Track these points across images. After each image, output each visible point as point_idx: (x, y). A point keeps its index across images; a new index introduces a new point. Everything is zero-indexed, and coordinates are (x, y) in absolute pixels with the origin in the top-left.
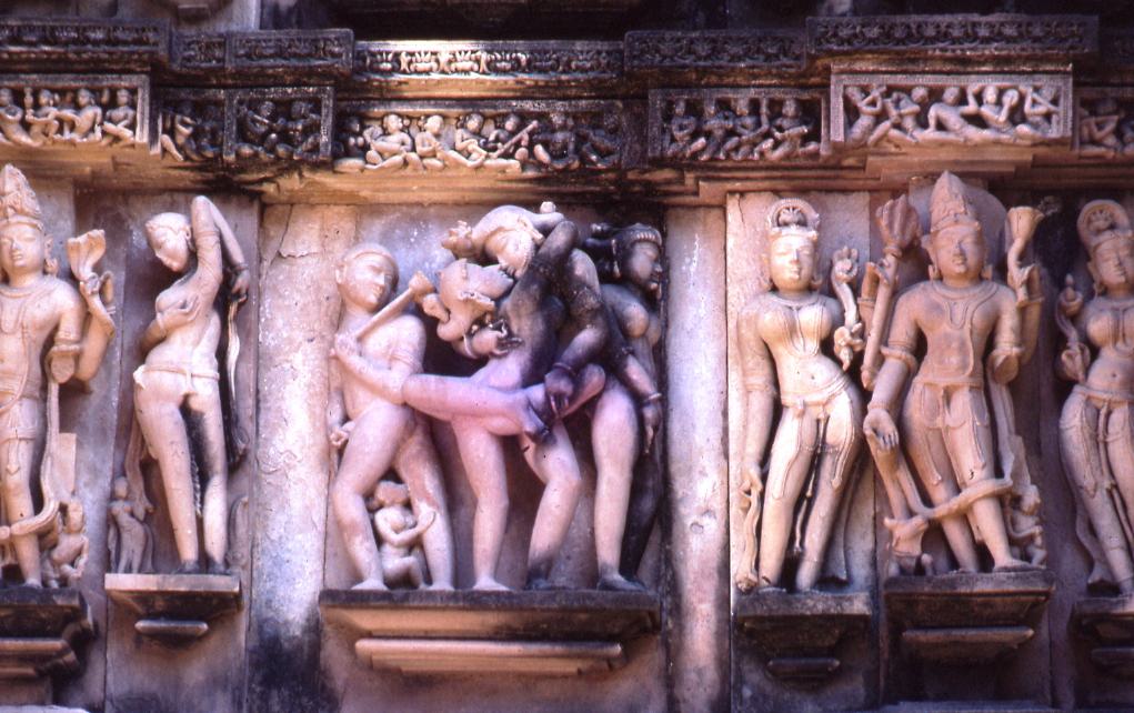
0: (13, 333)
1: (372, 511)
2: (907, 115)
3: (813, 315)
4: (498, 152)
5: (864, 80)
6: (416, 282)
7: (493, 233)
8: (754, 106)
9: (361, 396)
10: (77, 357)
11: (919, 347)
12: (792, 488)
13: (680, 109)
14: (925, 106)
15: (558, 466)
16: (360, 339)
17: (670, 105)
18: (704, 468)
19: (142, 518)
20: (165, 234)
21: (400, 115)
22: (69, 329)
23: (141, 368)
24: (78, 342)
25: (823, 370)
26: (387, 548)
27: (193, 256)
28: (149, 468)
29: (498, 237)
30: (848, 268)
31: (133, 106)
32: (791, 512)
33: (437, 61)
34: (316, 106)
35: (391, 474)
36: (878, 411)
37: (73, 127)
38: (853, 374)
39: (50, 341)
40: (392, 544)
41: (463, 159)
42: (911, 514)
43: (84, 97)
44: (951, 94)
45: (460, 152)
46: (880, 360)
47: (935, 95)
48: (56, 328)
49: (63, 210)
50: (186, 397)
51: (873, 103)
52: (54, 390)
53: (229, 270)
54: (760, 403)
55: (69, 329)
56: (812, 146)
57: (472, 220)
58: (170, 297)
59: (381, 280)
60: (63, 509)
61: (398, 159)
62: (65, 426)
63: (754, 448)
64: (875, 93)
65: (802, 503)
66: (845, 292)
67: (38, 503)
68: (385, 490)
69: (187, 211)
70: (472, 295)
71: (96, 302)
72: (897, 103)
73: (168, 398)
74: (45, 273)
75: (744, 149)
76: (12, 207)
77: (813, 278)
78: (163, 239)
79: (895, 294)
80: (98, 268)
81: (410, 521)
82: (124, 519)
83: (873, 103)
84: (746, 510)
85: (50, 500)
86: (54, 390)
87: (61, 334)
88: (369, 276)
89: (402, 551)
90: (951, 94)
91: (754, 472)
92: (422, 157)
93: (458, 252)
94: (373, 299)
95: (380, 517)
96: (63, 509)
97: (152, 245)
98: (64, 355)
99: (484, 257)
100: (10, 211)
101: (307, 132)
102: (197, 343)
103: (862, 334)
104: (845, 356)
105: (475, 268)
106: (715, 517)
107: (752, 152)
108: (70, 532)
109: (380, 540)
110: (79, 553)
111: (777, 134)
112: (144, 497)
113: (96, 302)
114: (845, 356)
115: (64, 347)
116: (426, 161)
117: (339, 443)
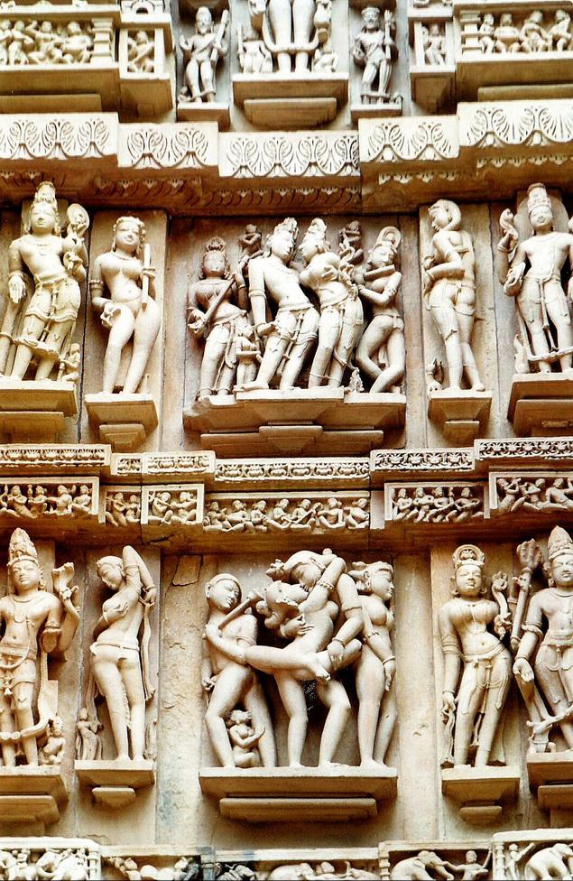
1: (228, 727)
2: (533, 494)
3: (483, 607)
4: (298, 521)
5: (509, 475)
6: (252, 596)
7: (296, 566)
8: (445, 491)
9: (221, 662)
11: (544, 624)
13: (402, 493)
14: (543, 488)
15: (337, 698)
16: (222, 627)
17: (397, 491)
19: (95, 731)
21: (241, 501)
22: (53, 621)
23: (95, 644)
25: (490, 638)
26: (237, 748)
27: (124, 579)
28: (101, 701)
29: (298, 569)
31: (90, 495)
32: (472, 721)
33: (263, 470)
34: (195, 493)
35: (240, 705)
36: (521, 661)
37: (55, 505)
38: (506, 642)
39: (43, 627)
40: (240, 746)
41: (277, 525)
42: (543, 720)
43: (62, 489)
44: (558, 483)
45: (276, 520)
46: (522, 632)
47: (549, 483)
48: (46, 620)
49: (49, 556)
50: (121, 659)
51: (514, 488)
53: (144, 589)
54: (453, 661)
55: (53, 621)
56: (479, 513)
57: (285, 556)
58: (111, 605)
59: (232, 595)
60: (51, 723)
61: (241, 525)
63: (450, 686)
64: (515, 482)
65: (477, 716)
66: (500, 597)
67: (37, 719)
68: (238, 715)
69: (120, 555)
72: (527, 488)
73: (109, 660)
74: (39, 589)
75: (439, 517)
77: (481, 590)
79: (528, 597)
80: (69, 585)
81: (250, 732)
82: (85, 732)
83: (514, 488)
84: (445, 722)
88: (227, 591)
89: (247, 750)
90: (558, 483)
91: (450, 698)
92: (255, 525)
93: (275, 577)
94: (228, 606)
95: (233, 730)
96: (51, 723)
97: (100, 575)
98: (50, 635)
99: (291, 579)
100: (19, 553)
101: (189, 509)
103: (510, 618)
104: (502, 632)
105: (286, 586)
107: (444, 518)
108: (55, 736)
109: (233, 743)
110: (60, 748)
111: (459, 508)
113: (69, 604)
114: (502, 632)
115: (51, 630)
116: (257, 527)
117: (209, 689)
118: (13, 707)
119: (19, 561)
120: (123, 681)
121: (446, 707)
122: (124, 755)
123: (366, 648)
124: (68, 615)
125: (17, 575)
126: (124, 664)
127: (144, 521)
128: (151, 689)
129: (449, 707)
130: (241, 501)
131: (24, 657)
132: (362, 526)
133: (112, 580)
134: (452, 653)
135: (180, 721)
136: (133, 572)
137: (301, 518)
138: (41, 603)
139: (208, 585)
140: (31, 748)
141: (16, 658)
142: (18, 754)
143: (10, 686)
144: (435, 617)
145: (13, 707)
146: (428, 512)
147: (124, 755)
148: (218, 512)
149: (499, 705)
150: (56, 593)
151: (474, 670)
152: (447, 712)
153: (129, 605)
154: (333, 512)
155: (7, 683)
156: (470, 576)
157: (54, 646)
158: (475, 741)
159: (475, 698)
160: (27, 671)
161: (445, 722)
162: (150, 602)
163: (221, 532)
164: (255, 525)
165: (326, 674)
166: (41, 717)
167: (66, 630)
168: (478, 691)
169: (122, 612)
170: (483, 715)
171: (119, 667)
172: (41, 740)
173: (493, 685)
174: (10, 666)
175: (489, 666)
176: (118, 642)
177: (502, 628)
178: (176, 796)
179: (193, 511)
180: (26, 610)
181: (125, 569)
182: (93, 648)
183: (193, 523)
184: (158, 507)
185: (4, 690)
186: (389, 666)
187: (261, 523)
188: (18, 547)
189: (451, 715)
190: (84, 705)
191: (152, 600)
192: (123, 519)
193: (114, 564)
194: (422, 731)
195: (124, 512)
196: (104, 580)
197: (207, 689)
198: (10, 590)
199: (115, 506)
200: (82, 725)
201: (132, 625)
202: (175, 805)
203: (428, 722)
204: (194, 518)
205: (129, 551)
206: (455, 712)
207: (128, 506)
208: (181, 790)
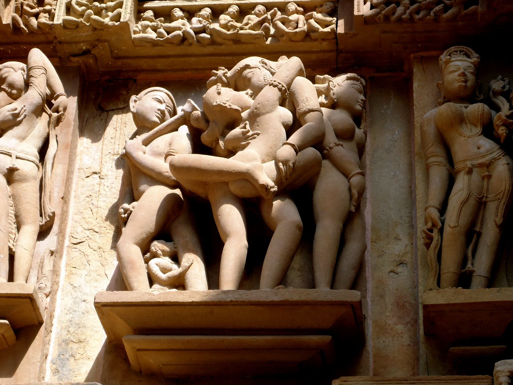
1: (147, 261)
12: (464, 220)
18: (398, 235)
21: (182, 9)
25: (486, 144)
29: (246, 72)
30: (502, 86)
54: (438, 175)
65: (471, 235)
69: (23, 58)
70: (225, 104)
91: (435, 214)
101: (113, 9)
102: (22, 138)
106: (407, 267)
107: (429, 14)
117: (126, 215)
121: (430, 225)
123: (326, 163)
127: (58, 20)
128: (49, 209)
129: (434, 225)
130: (182, 9)
132: (328, 29)
134: (439, 164)
135: (90, 258)
137: (252, 23)
139: (133, 97)
144: (417, 134)
146: (408, 8)
148: (151, 21)
149: (499, 220)
151: (466, 177)
152: (431, 230)
154: (293, 17)
156: (462, 70)
158: (469, 265)
159: (468, 209)
161: (428, 246)
162: (58, 112)
163: (153, 43)
164: (197, 32)
165: (271, 183)
168: (472, 201)
170: (479, 234)
173: (491, 196)
175: (487, 173)
177: (503, 128)
178: (75, 346)
179: (115, 12)
183: (117, 24)
184: (77, 7)
186: (356, 180)
187: (204, 30)
189: (435, 234)
192: (34, 21)
194: (400, 269)
195: (36, 16)
197: (123, 216)
199: (25, 7)
202: (72, 356)
203: (408, 259)
204: (117, 18)
205: (37, 56)
206: (441, 231)
207: (41, 8)
208: (82, 337)
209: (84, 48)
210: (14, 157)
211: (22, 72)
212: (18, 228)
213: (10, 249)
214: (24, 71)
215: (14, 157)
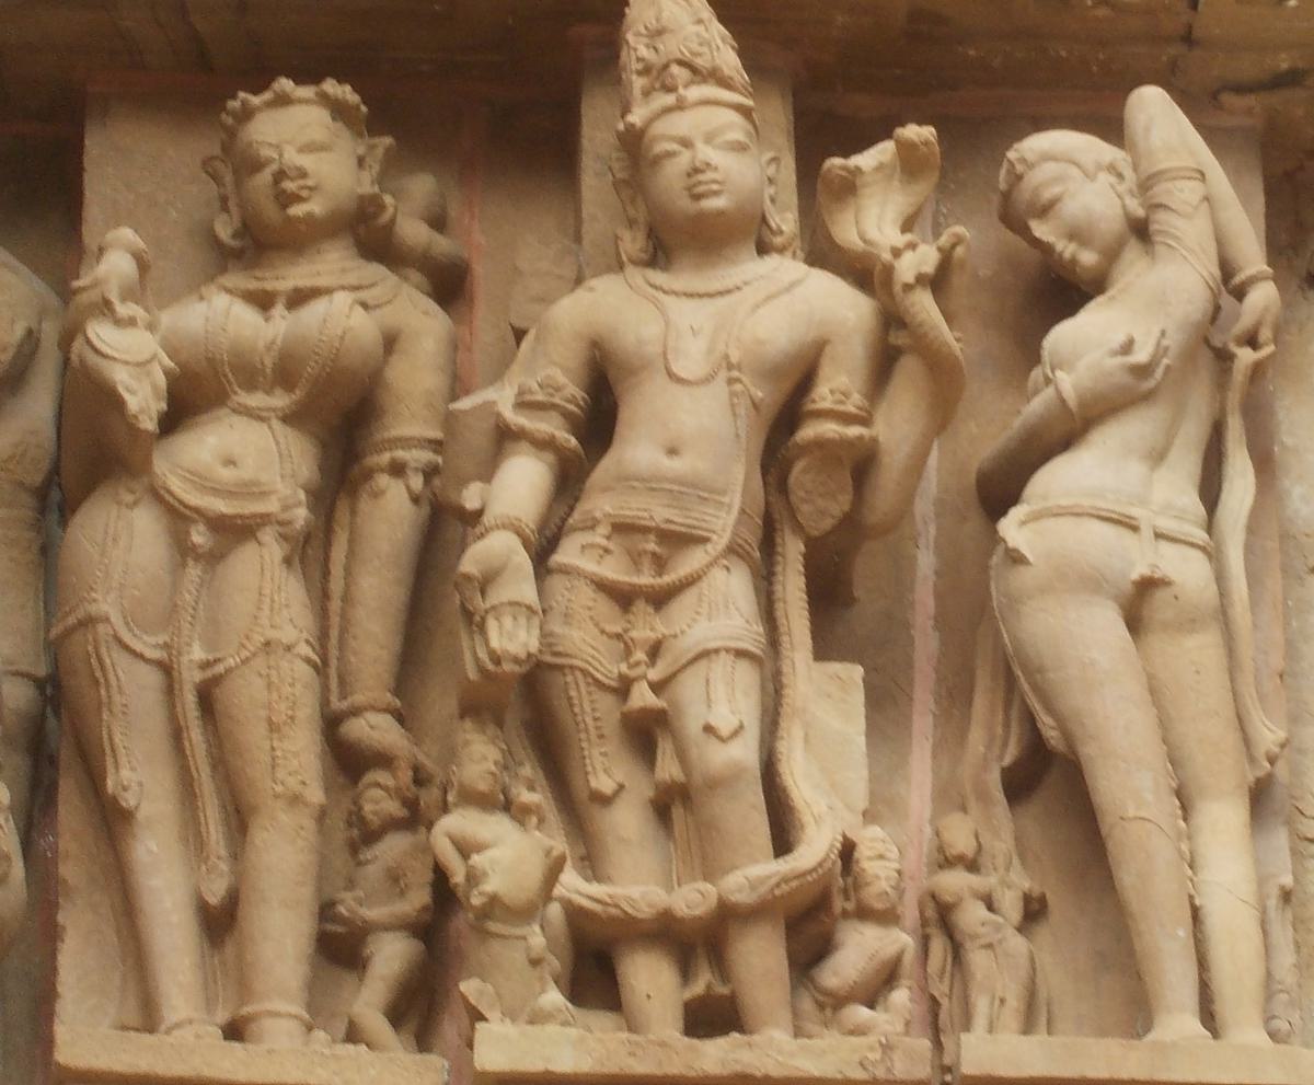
0: (708, 379)
10: (862, 464)
20: (1058, 179)
23: (1016, 513)
24: (865, 421)
27: (1140, 230)
48: (805, 381)
50: (1148, 586)
52: (793, 550)
55: (838, 385)
58: (1085, 344)
60: (848, 851)
62: (824, 649)
67: (783, 832)
71: (924, 306)
73: (1091, 582)
74: (763, 249)
76: (681, 63)
78: (1056, 190)
82: (972, 916)
85: (818, 820)
86: (793, 550)
87: (824, 394)
96: (848, 851)
102: (1157, 456)
108: (864, 914)
112: (1016, 861)
113: (924, 306)
115: (830, 429)
118: (668, 768)
119: (680, 106)
120: (1154, 691)
122: (1179, 1023)
124: (909, 372)
125: (671, 177)
126: (1160, 607)
128: (1268, 734)
131: (720, 542)
133: (1076, 235)
136: (1185, 193)
138: (786, 301)
140: (760, 959)
141: (678, 540)
142: (698, 988)
143: (655, 674)
145: (668, 768)
147: (1179, 1023)
150: (863, 272)
153: (1173, 341)
155: (640, 655)
157: (841, 504)
160: (720, 609)
162: (1252, 341)
166: (806, 817)
167: (896, 426)
169: (1142, 371)
171: (1135, 622)
172: (808, 923)
174: (646, 579)
176: (1107, 506)
180: (715, 335)
181: (1145, 185)
182: (1012, 528)
185: (623, 689)
188: (671, 47)
190: (948, 797)
191: (1265, 334)
193: (1088, 160)
196: (1040, 230)
198: (632, 243)
200: (954, 882)
201: (1178, 441)
209: (1284, 66)
210: (1147, 532)
211: (1113, 179)
212: (1186, 810)
213: (1191, 897)
214: (1120, 176)
215: (1147, 532)
